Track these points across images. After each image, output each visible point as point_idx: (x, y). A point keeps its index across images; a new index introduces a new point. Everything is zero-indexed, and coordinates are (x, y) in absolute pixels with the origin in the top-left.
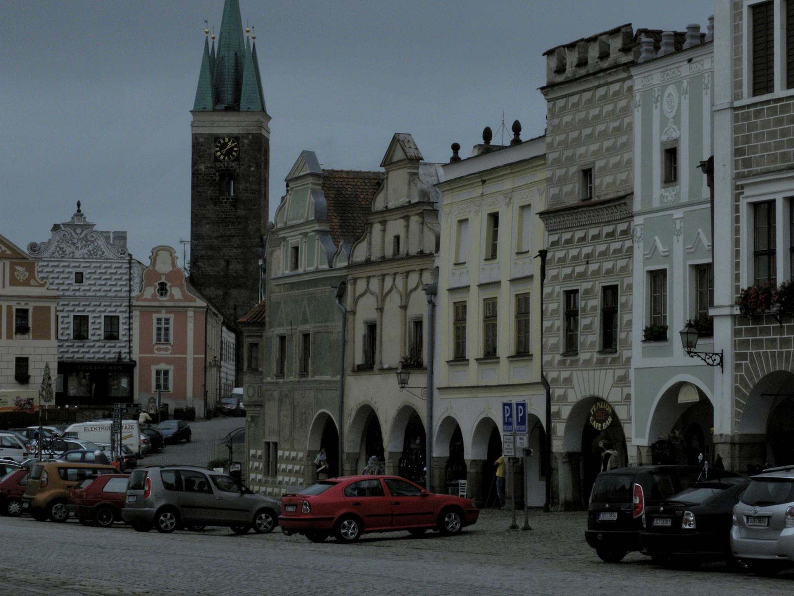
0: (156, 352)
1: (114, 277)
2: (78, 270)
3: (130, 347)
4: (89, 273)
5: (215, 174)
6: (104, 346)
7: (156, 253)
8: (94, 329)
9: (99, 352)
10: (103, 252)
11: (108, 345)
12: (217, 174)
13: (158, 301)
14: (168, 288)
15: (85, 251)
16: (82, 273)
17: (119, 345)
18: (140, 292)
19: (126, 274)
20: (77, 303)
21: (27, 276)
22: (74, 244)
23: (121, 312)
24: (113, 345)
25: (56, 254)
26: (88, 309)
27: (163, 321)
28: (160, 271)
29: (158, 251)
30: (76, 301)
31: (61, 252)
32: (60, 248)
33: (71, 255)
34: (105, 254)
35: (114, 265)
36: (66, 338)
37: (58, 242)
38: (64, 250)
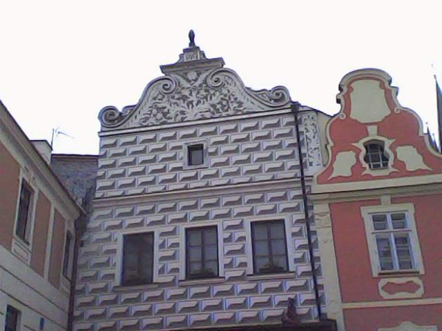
0: (383, 294)
1: (266, 144)
3: (317, 287)
4: (215, 143)
6: (254, 291)
8: (230, 252)
9: (243, 306)
10: (240, 104)
11: (265, 285)
14: (387, 149)
15: (205, 106)
17: (290, 284)
18: (324, 166)
20: (192, 203)
22: (184, 98)
24: (276, 284)
25: (152, 120)
26: (215, 212)
29: (351, 83)
30: (188, 199)
31: (160, 115)
32: (159, 109)
34: (244, 106)
35: (265, 122)
36: (170, 279)
37: (155, 99)
38: (166, 110)
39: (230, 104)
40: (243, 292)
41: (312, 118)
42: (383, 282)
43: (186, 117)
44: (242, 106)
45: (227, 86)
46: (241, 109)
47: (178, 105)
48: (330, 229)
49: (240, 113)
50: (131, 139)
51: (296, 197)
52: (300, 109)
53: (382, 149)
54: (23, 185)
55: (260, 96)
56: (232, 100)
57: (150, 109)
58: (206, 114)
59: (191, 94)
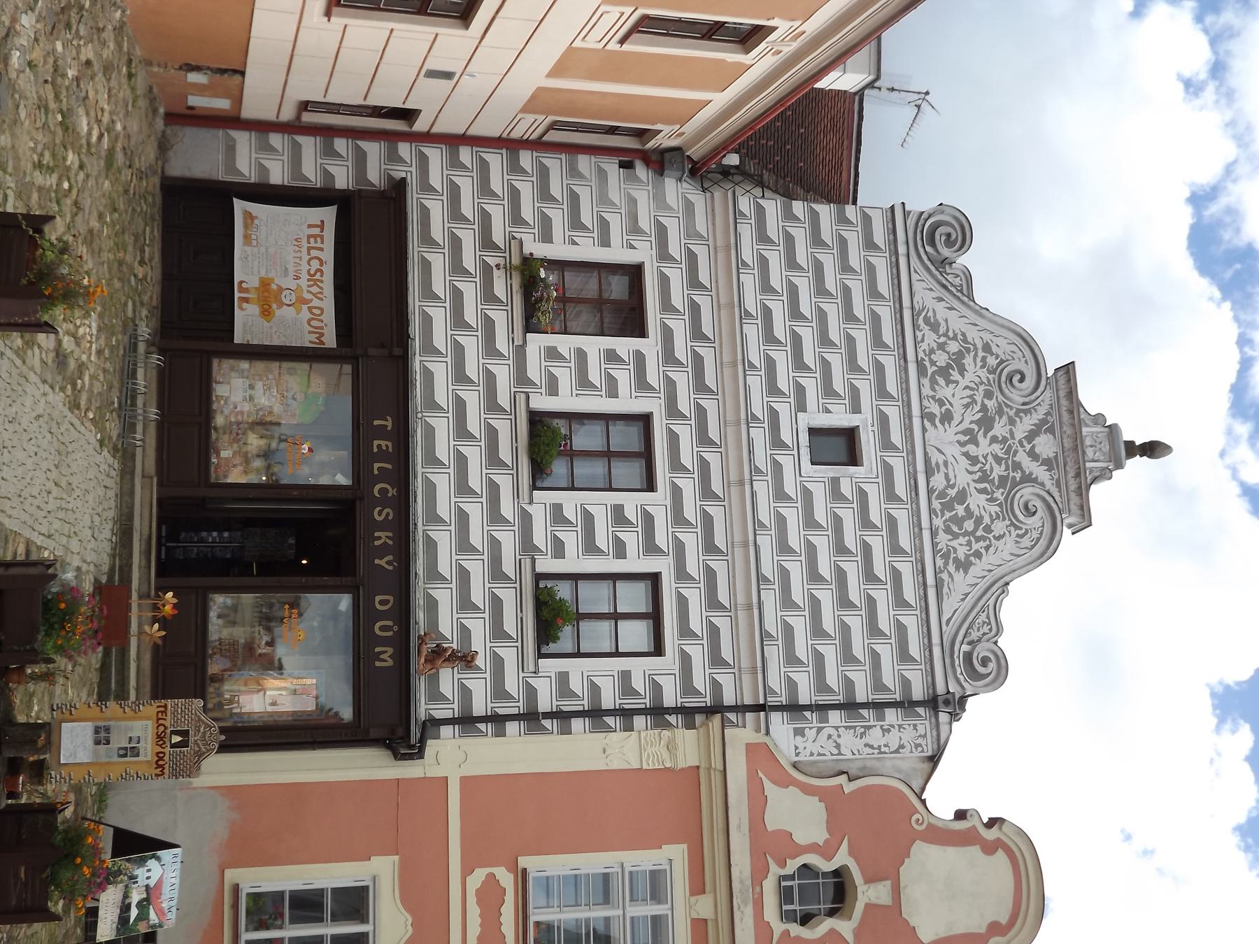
1: (856, 623)
2: (868, 443)
3: (498, 720)
4: (863, 495)
6: (497, 573)
8: (588, 519)
9: (464, 545)
10: (964, 566)
13: (759, 874)
14: (828, 924)
15: (963, 478)
17: (509, 655)
18: (795, 766)
19: (879, 686)
22: (986, 422)
23: (686, 659)
25: (930, 339)
28: (907, 872)
30: (723, 423)
31: (941, 359)
32: (959, 356)
34: (959, 576)
35: (911, 623)
36: (533, 372)
37: (987, 348)
38: (955, 375)
39: (962, 540)
40: (495, 545)
41: (917, 746)
43: (936, 427)
44: (957, 569)
45: (1014, 533)
46: (951, 568)
47: (967, 406)
48: (636, 766)
49: (940, 562)
50: (883, 286)
51: (716, 687)
52: (943, 717)
53: (831, 913)
54: (762, 27)
55: (983, 617)
56: (975, 546)
57: (960, 337)
59: (994, 440)
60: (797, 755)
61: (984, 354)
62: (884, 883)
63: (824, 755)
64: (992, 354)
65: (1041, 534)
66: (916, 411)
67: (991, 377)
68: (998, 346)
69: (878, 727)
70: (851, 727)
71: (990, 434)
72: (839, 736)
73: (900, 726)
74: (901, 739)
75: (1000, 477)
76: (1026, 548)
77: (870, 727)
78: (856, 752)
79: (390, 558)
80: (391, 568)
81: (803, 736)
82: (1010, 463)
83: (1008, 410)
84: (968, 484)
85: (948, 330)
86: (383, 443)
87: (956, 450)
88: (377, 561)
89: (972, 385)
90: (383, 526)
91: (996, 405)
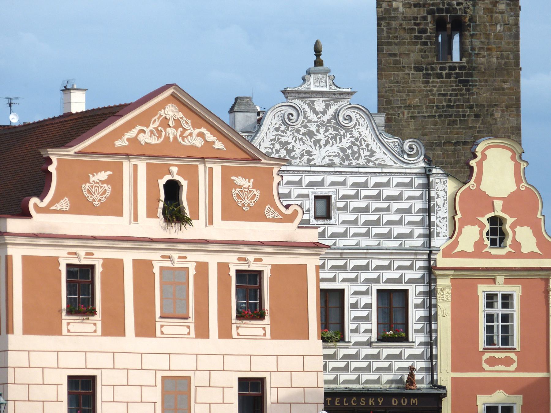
0: (485, 366)
4: (344, 197)
5: (425, 18)
6: (377, 356)
7: (483, 153)
8: (356, 318)
9: (367, 369)
10: (372, 153)
12: (429, 17)
13: (489, 256)
14: (507, 227)
15: (334, 149)
16: (328, 198)
17: (408, 352)
18: (451, 238)
21: (257, 198)
22: (310, 134)
23: (411, 281)
24: (397, 352)
26: (342, 275)
27: (500, 301)
33: (305, 158)
34: (377, 156)
35: (396, 180)
37: (277, 129)
38: (290, 147)
39: (361, 152)
40: (367, 357)
41: (444, 184)
42: (486, 356)
43: (313, 159)
44: (374, 156)
45: (358, 127)
46: (373, 159)
47: (304, 143)
49: (371, 164)
51: (420, 268)
53: (501, 224)
55: (392, 145)
56: (364, 146)
58: (334, 158)
59: (318, 131)
60: (447, 236)
61: (280, 131)
62: (495, 204)
63: (447, 224)
64: (280, 127)
65: (358, 113)
66: (308, 169)
67: (290, 129)
68: (276, 123)
69: (437, 200)
70: (437, 212)
71: (315, 132)
72: (440, 217)
73: (436, 190)
74: (441, 190)
75: (334, 130)
76: (364, 121)
77: (437, 203)
78: (446, 211)
79: (379, 399)
80: (382, 399)
81: (439, 233)
82: (328, 125)
83: (305, 122)
84: (338, 146)
85: (270, 148)
86: (336, 402)
87: (323, 150)
88: (380, 404)
89: (294, 139)
90: (367, 402)
91: (302, 128)
